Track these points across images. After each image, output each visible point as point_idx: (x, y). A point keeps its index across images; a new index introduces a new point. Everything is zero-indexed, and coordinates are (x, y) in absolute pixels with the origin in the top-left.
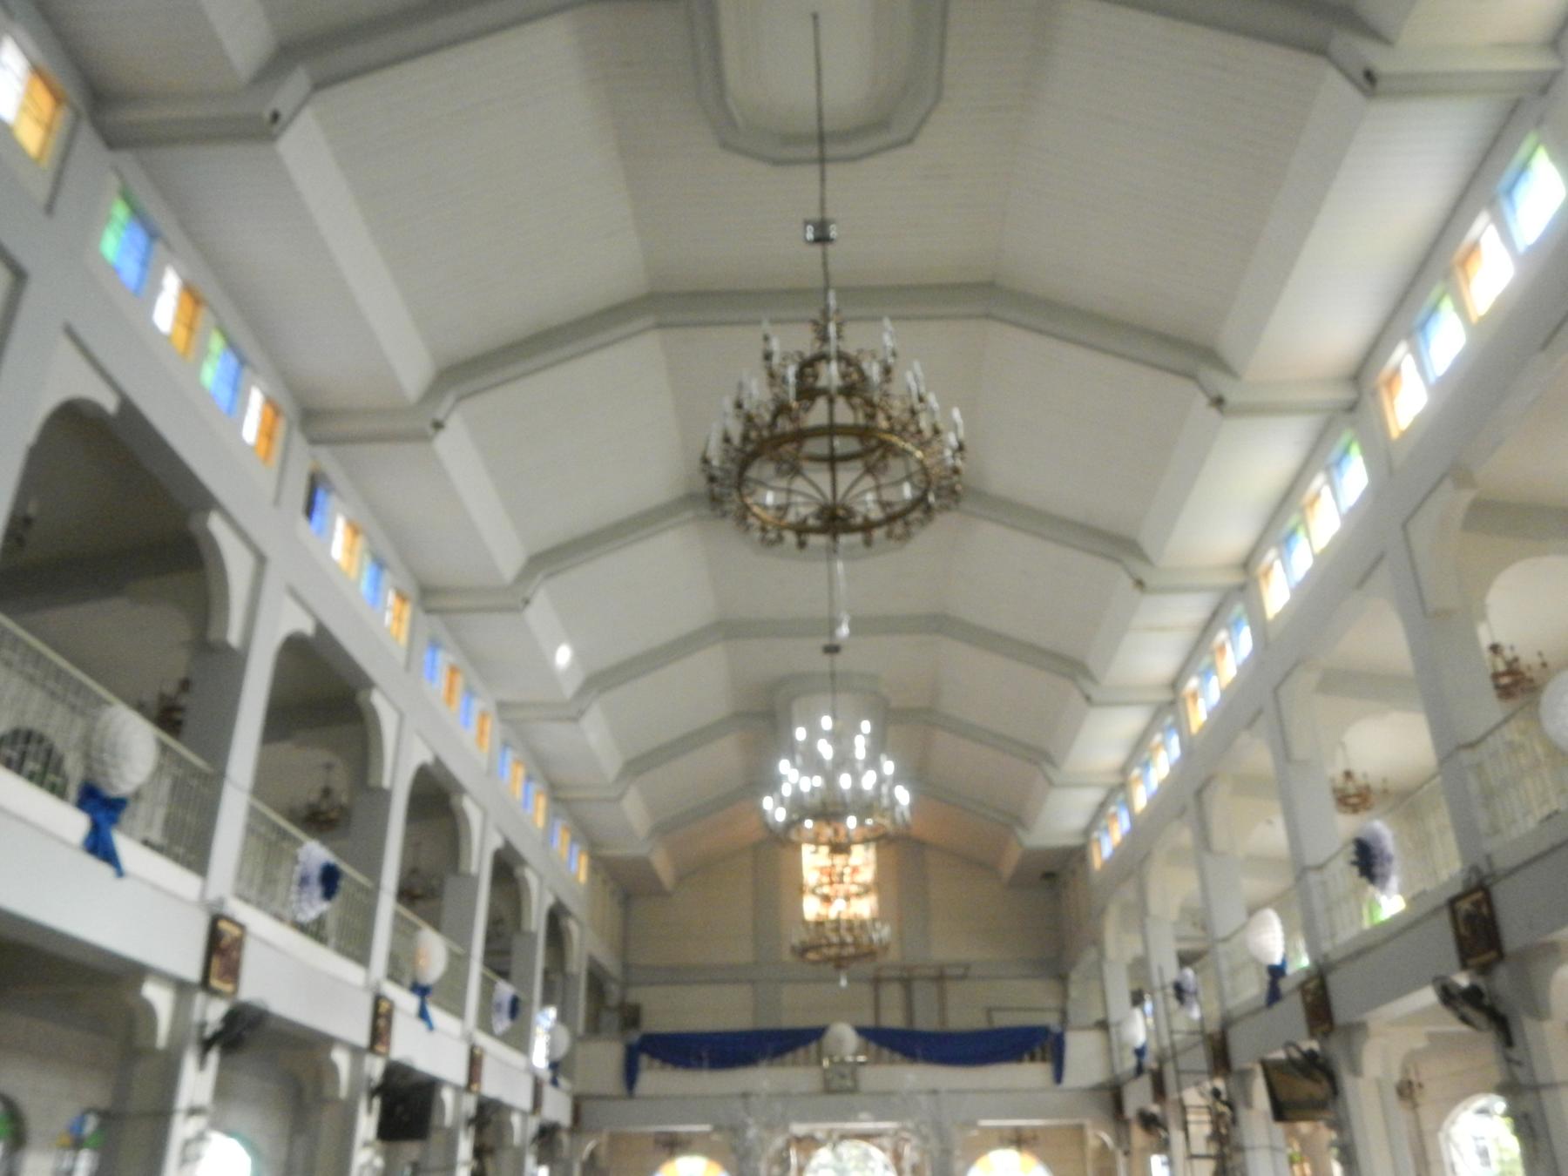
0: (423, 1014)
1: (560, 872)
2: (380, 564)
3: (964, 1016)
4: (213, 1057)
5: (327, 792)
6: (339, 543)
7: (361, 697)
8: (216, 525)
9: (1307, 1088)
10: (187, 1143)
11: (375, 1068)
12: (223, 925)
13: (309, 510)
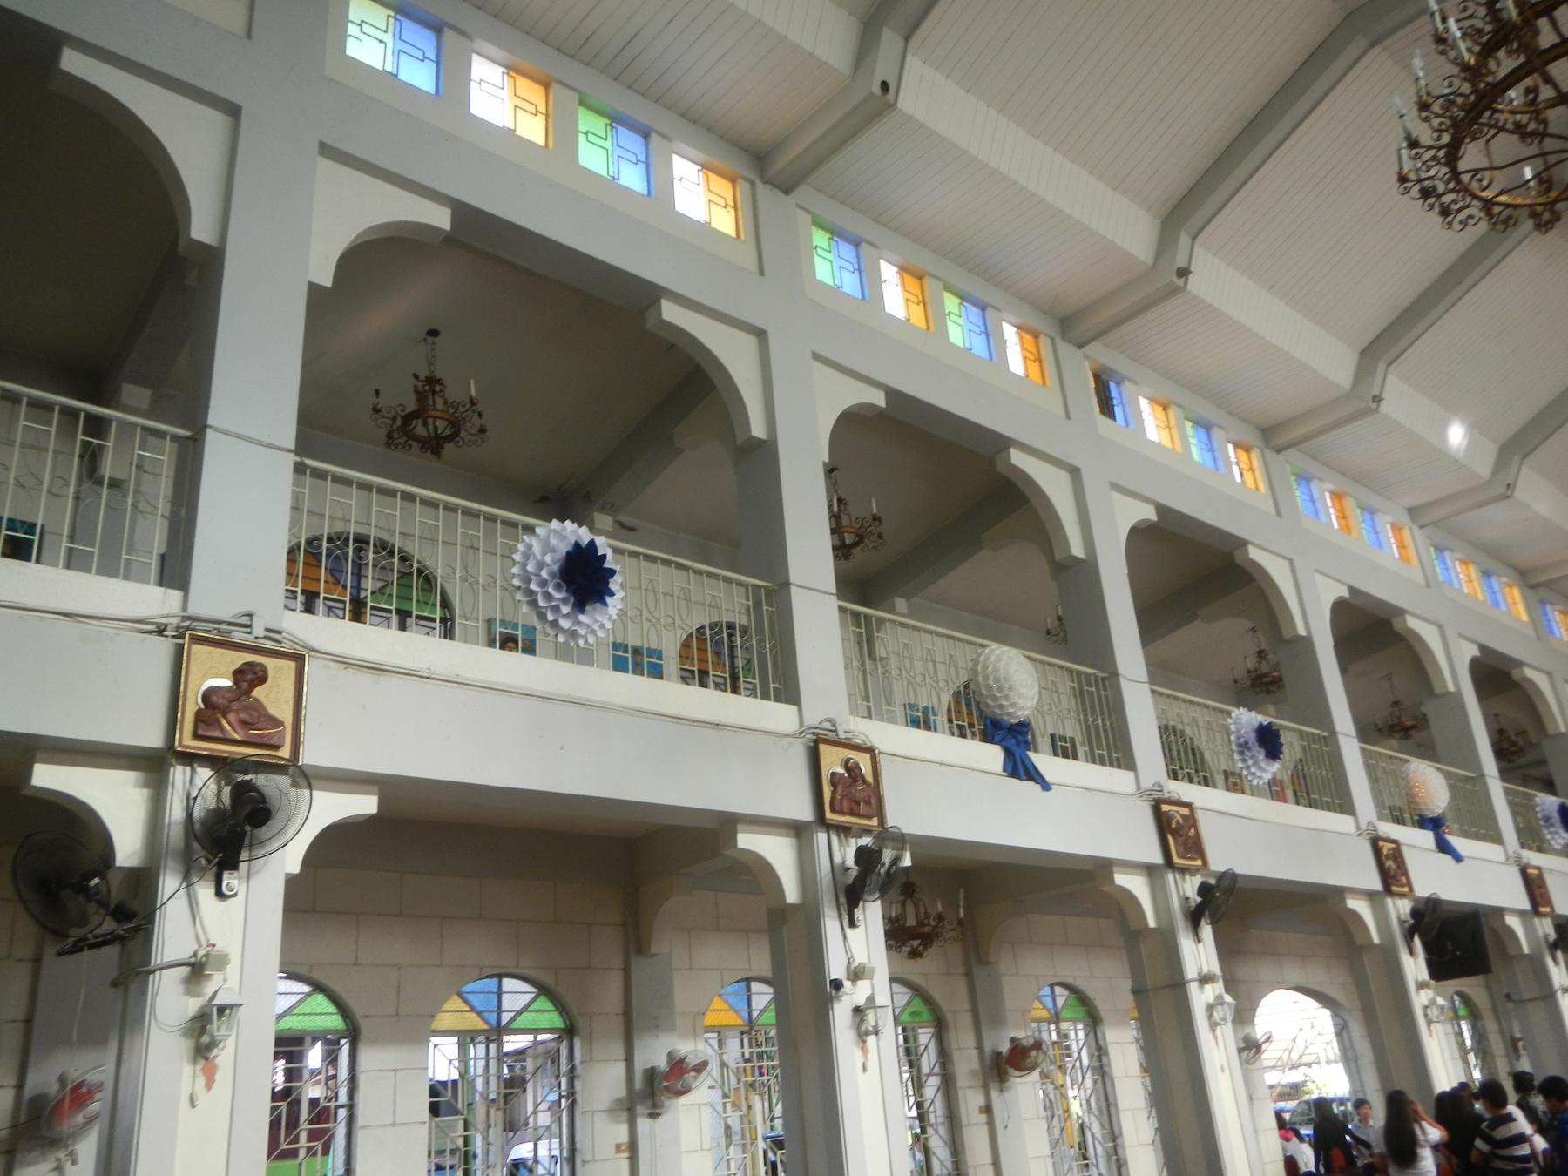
2: (1205, 426)
4: (1207, 931)
6: (1152, 424)
7: (1238, 559)
8: (1018, 458)
10: (1210, 1008)
11: (1400, 908)
13: (1107, 408)
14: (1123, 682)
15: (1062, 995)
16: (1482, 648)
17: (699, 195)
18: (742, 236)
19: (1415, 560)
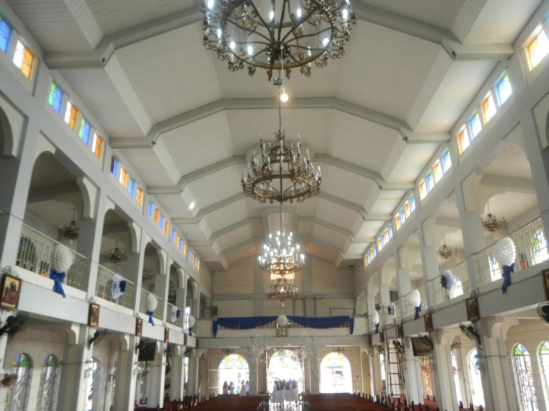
0: (151, 321)
1: (192, 267)
2: (134, 181)
3: (322, 313)
5: (117, 249)
6: (122, 178)
7: (129, 225)
8: (85, 181)
9: (424, 346)
10: (86, 371)
11: (137, 340)
12: (93, 306)
13: (112, 170)
15: (23, 357)
16: (175, 262)
18: (31, 79)
19: (168, 233)
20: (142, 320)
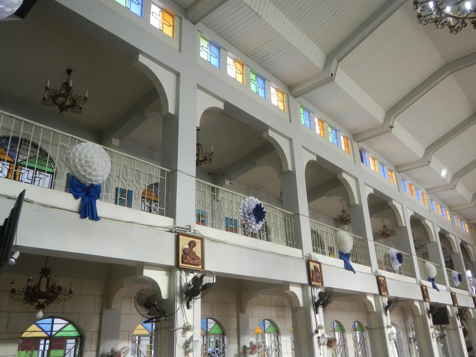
0: (434, 287)
1: (460, 231)
2: (383, 165)
5: (384, 226)
6: (372, 165)
7: (389, 203)
8: (344, 175)
11: (427, 305)
12: (380, 278)
13: (362, 161)
14: (369, 241)
16: (441, 229)
17: (276, 98)
18: (286, 111)
19: (427, 204)
20: (426, 286)
